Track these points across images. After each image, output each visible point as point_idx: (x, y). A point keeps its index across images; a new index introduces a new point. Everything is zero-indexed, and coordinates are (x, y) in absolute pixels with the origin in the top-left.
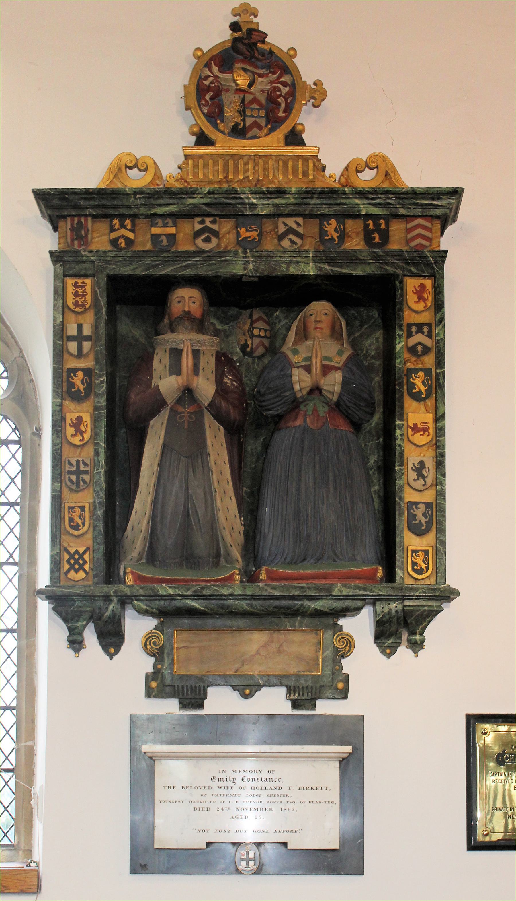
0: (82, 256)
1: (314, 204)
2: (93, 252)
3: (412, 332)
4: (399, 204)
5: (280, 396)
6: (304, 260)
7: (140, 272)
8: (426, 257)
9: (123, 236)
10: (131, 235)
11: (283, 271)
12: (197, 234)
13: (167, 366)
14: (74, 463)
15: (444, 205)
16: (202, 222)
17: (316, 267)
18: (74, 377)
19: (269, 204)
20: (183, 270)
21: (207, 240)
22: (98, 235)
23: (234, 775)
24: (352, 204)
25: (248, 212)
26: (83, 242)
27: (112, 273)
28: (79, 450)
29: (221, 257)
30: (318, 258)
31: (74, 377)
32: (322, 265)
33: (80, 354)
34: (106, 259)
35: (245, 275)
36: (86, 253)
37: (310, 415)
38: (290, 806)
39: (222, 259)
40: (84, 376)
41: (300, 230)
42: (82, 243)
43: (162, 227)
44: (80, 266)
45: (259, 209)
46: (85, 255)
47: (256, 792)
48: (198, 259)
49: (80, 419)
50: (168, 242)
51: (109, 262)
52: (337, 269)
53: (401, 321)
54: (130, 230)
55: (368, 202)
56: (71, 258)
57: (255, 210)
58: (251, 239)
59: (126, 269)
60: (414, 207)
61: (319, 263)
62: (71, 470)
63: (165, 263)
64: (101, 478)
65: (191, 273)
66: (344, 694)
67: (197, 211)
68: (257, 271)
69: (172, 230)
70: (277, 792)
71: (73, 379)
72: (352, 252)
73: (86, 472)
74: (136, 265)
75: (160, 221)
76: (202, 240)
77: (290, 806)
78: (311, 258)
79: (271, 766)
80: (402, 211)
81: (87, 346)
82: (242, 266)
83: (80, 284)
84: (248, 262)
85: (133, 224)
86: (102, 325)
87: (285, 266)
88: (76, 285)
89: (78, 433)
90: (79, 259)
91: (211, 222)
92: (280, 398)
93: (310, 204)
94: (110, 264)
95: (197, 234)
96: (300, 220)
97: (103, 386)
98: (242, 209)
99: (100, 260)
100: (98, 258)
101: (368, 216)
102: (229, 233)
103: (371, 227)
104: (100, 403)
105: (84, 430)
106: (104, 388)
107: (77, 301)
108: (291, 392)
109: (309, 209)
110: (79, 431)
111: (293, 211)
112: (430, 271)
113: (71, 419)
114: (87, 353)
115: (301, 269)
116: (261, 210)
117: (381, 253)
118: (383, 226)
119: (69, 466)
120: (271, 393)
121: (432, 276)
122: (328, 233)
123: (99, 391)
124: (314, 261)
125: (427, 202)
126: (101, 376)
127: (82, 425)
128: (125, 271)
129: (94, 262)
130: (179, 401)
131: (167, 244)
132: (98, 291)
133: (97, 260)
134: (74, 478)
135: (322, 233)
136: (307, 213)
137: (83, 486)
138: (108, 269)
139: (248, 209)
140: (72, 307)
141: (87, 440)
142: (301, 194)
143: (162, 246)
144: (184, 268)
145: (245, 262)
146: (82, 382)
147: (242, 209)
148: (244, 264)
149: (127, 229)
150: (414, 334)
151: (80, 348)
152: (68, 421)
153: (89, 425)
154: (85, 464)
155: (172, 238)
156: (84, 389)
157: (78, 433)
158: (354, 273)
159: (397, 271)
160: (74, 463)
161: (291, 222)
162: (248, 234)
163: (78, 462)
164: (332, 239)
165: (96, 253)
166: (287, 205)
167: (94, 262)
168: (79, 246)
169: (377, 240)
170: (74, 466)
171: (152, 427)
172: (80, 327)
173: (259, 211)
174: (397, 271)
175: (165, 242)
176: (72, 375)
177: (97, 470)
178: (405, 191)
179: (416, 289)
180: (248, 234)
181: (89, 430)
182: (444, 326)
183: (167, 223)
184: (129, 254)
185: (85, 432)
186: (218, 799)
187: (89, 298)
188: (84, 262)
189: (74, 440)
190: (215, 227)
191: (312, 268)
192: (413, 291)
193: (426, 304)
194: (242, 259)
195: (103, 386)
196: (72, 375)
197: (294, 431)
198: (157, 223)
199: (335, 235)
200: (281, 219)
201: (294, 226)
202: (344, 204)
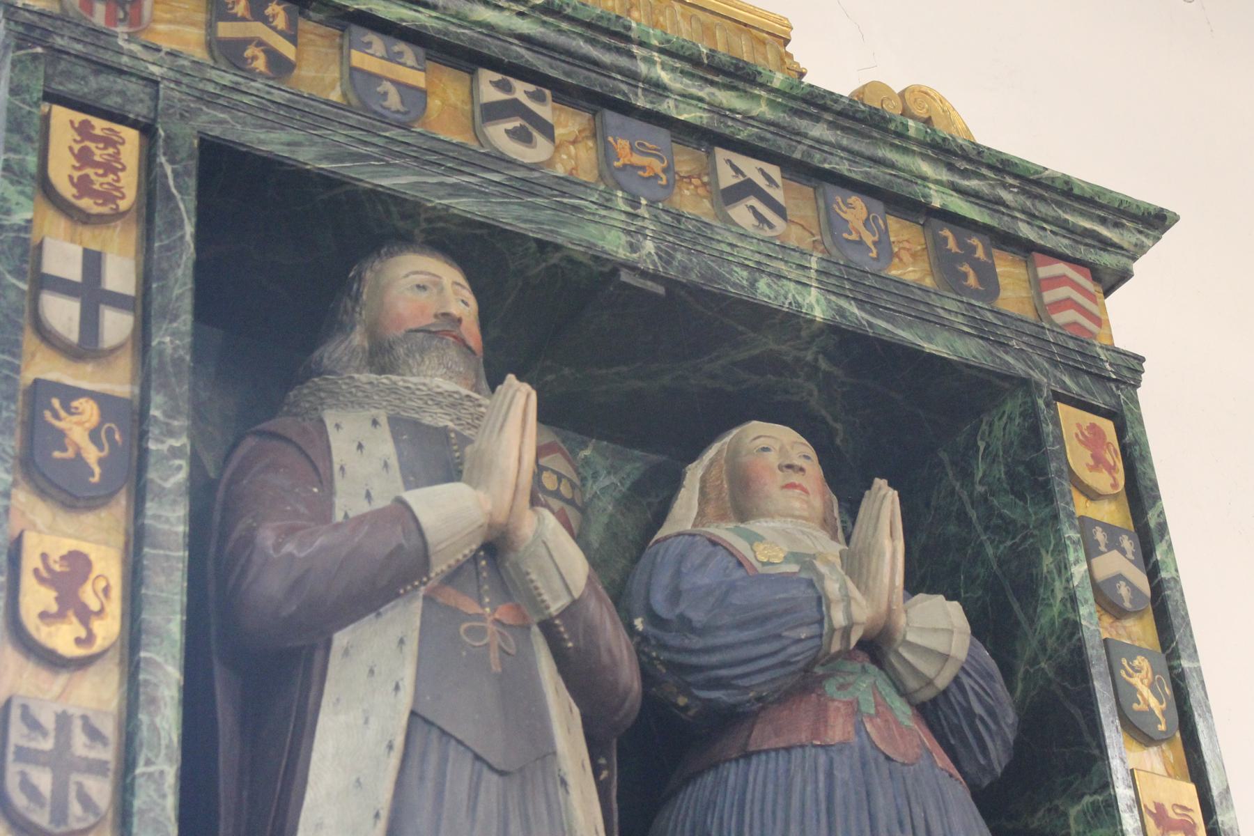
0: (120, 52)
1: (818, 141)
2: (158, 50)
3: (1097, 543)
4: (1023, 212)
5: (779, 637)
6: (795, 274)
7: (309, 156)
8: (1096, 358)
9: (260, 43)
10: (286, 49)
11: (743, 287)
12: (493, 112)
13: (394, 462)
14: (47, 720)
15: (1126, 245)
16: (503, 86)
17: (829, 301)
18: (63, 413)
19: (701, 100)
20: (450, 195)
21: (521, 136)
22: (168, 16)
24: (911, 172)
25: (641, 102)
26: (126, 14)
27: (216, 131)
28: (63, 678)
29: (563, 194)
30: (832, 281)
31: (63, 413)
32: (843, 303)
33: (87, 349)
34: (201, 86)
35: (633, 268)
36: (135, 48)
37: (870, 717)
39: (565, 200)
40: (104, 417)
41: (778, 195)
42: (121, 15)
43: (382, 58)
44: (105, 81)
45: (671, 103)
46: (131, 51)
48: (496, 177)
49: (78, 564)
50: (402, 102)
51: (209, 100)
52: (884, 324)
53: (1067, 504)
54: (281, 33)
55: (951, 179)
56: (79, 47)
57: (661, 103)
58: (646, 175)
59: (262, 135)
60: (1054, 229)
61: (834, 293)
62: (33, 745)
63: (393, 154)
64: (164, 796)
65: (475, 209)
67: (493, 48)
68: (668, 263)
69: (417, 79)
71: (56, 416)
72: (919, 292)
73: (96, 768)
74: (298, 136)
75: (377, 42)
76: (507, 131)
78: (813, 274)
80: (1026, 231)
81: (116, 326)
82: (624, 239)
83: (97, 132)
84: (640, 231)
85: (292, 23)
86: (180, 272)
87: (745, 274)
88: (84, 131)
89: (70, 613)
90: (108, 57)
91: (531, 95)
92: (775, 645)
93: (805, 136)
94: (208, 103)
95: (493, 112)
96: (774, 171)
97: (179, 468)
98: (624, 87)
99: (178, 83)
100: (171, 74)
101: (946, 216)
102: (574, 142)
103: (952, 244)
104: (167, 520)
105: (94, 605)
106: (182, 476)
107: (85, 180)
108: (814, 629)
109: (800, 147)
110: (70, 603)
111: (762, 139)
112: (1108, 399)
113: (44, 557)
114: (113, 350)
115: (790, 296)
116: (677, 107)
117: (990, 317)
118: (980, 253)
119: (25, 730)
120: (741, 626)
121: (1114, 415)
122: (850, 226)
123: (166, 480)
124: (820, 282)
125: (1087, 224)
126: (171, 433)
127: (88, 587)
128: (261, 142)
129: (156, 83)
130: (453, 576)
131: (400, 107)
132: (168, 169)
133: (169, 80)
134: (43, 780)
135: (832, 224)
136: (797, 155)
137: (79, 820)
138: (204, 118)
139: (640, 91)
140: (67, 190)
141: (107, 644)
142: (794, 98)
143: (382, 106)
144: (450, 191)
145: (633, 228)
146: (94, 436)
147: (624, 87)
148: (628, 233)
149: (274, 29)
150: (1102, 548)
151: (90, 323)
152: (30, 561)
153: (116, 592)
154: (94, 734)
155: (416, 97)
156: (101, 462)
157: (70, 613)
158: (929, 347)
159: (1031, 372)
160: (47, 720)
161: (751, 168)
162: (637, 159)
163: (63, 721)
164: (860, 242)
165: (168, 59)
166: (747, 118)
167: (156, 83)
168: (111, 19)
169: (972, 281)
170: (45, 734)
171: (346, 653)
172: (93, 262)
173: (668, 107)
174: (1031, 372)
175: (394, 100)
176: (56, 403)
177: (148, 762)
178: (1047, 178)
179: (1083, 434)
180: (637, 159)
181: (115, 608)
182: (1170, 546)
183: (400, 54)
184: (278, 96)
185: (100, 613)
187: (129, 182)
188: (120, 72)
189: (50, 635)
190: (545, 111)
191: (818, 301)
192: (1077, 435)
193: (1114, 478)
194: (623, 217)
195: (179, 468)
196: (56, 403)
197: (822, 759)
198: (369, 45)
199: (869, 239)
200: (721, 154)
201: (761, 182)
202: (892, 166)
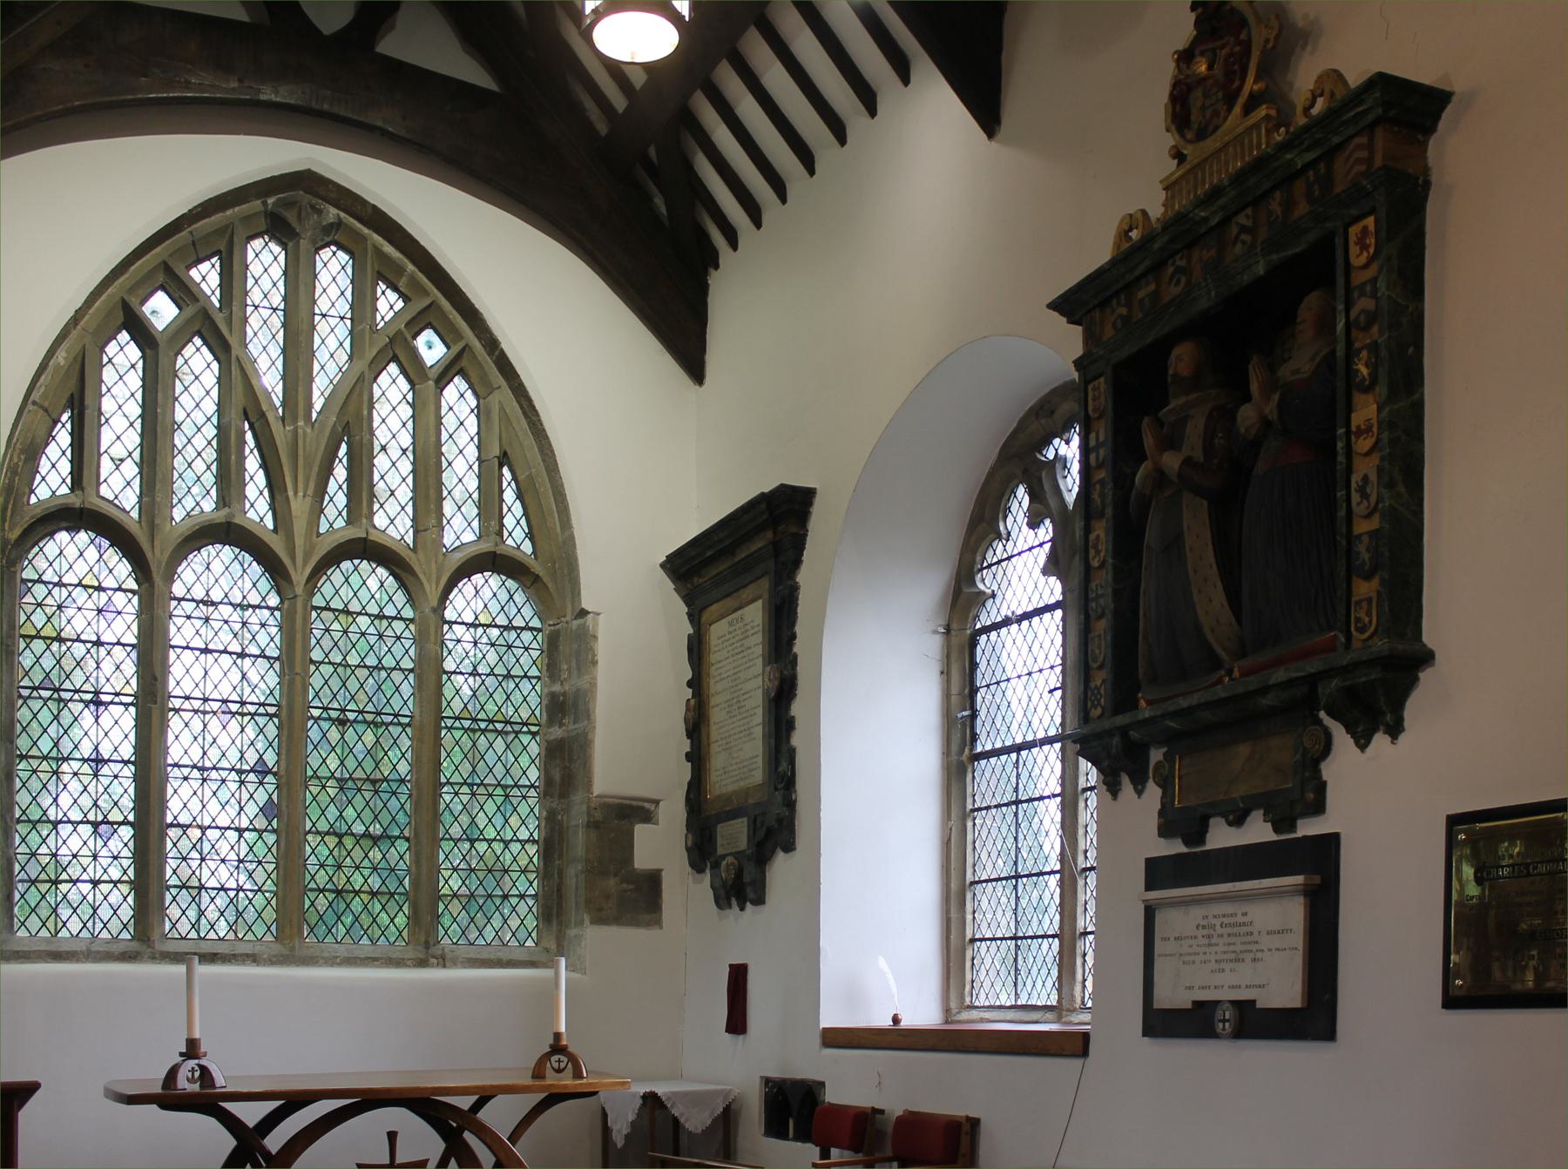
23: (1214, 921)
38: (1259, 955)
47: (1232, 940)
66: (1318, 807)
70: (1249, 938)
77: (1259, 955)
79: (1246, 907)
186: (1201, 950)
